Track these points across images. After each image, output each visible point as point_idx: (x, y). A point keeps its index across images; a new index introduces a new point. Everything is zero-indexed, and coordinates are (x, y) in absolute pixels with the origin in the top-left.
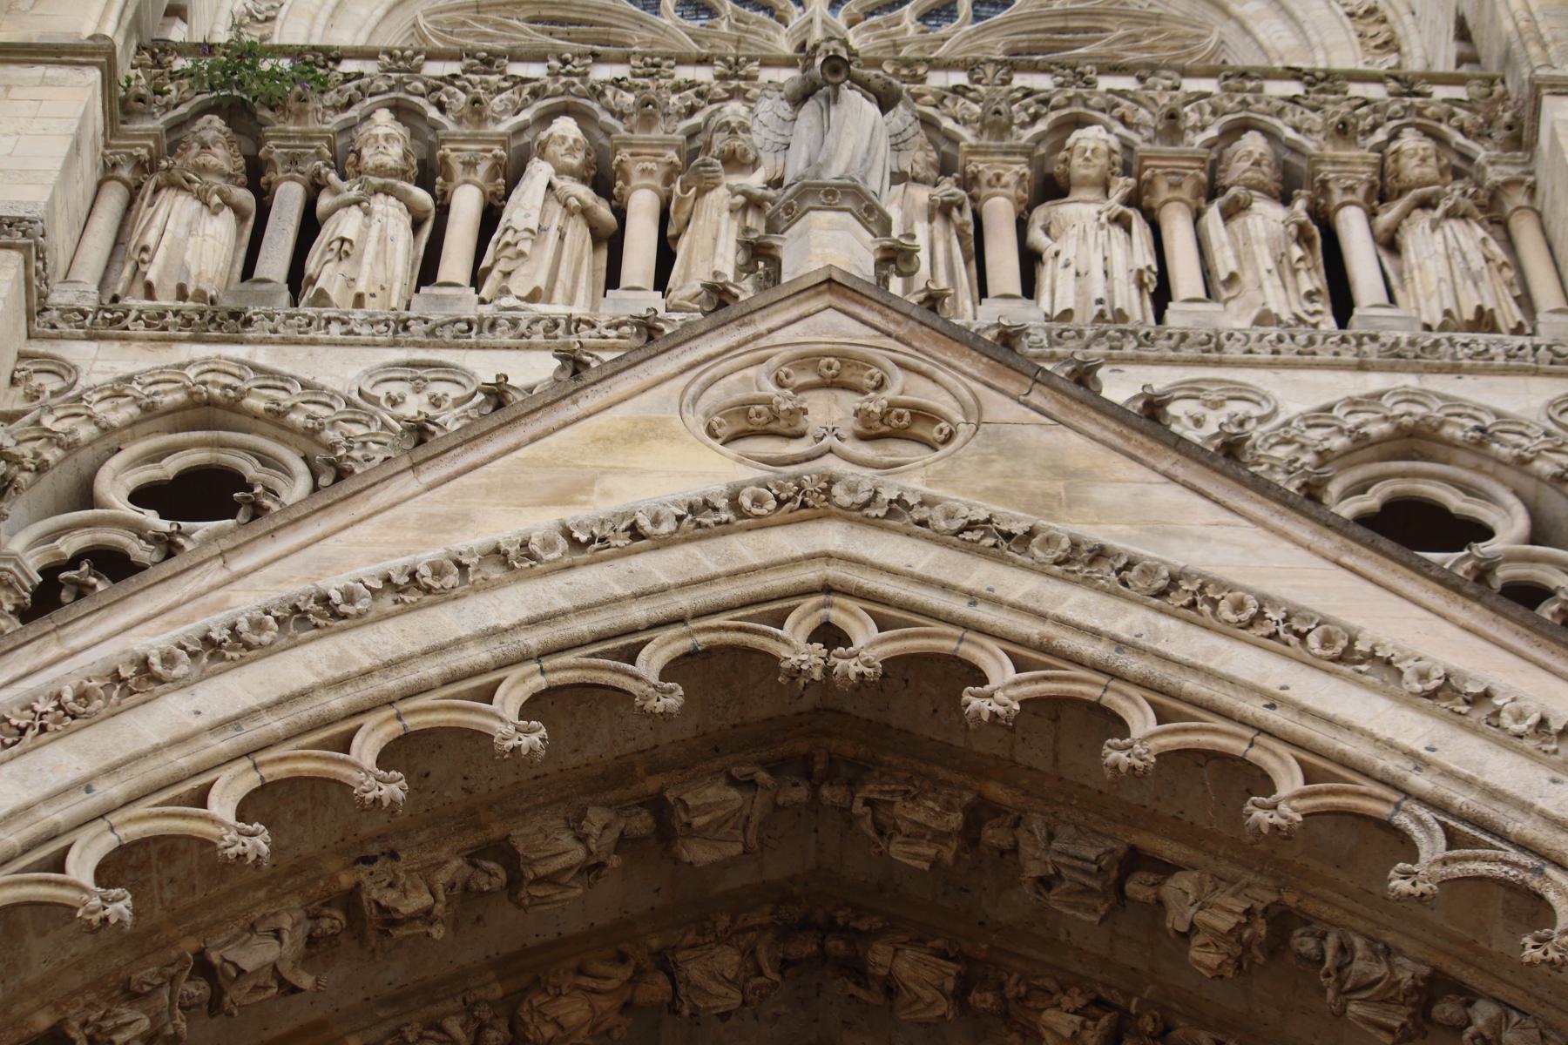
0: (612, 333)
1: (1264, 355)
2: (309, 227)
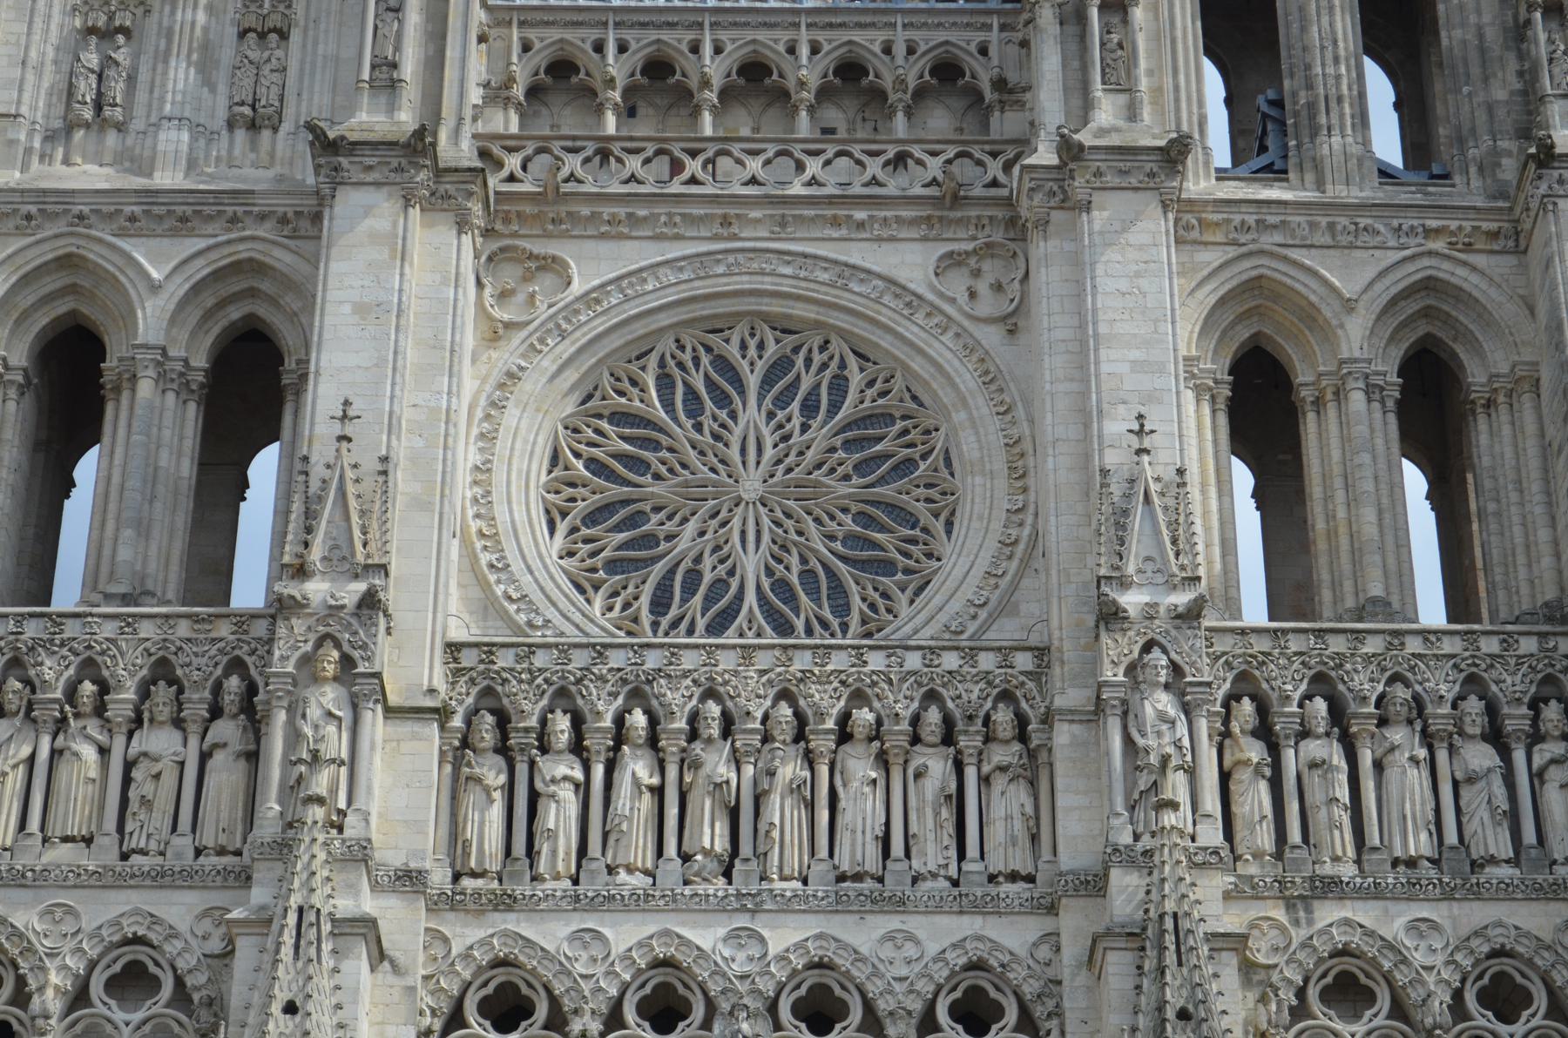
0: (661, 903)
1: (922, 909)
2: (534, 797)
